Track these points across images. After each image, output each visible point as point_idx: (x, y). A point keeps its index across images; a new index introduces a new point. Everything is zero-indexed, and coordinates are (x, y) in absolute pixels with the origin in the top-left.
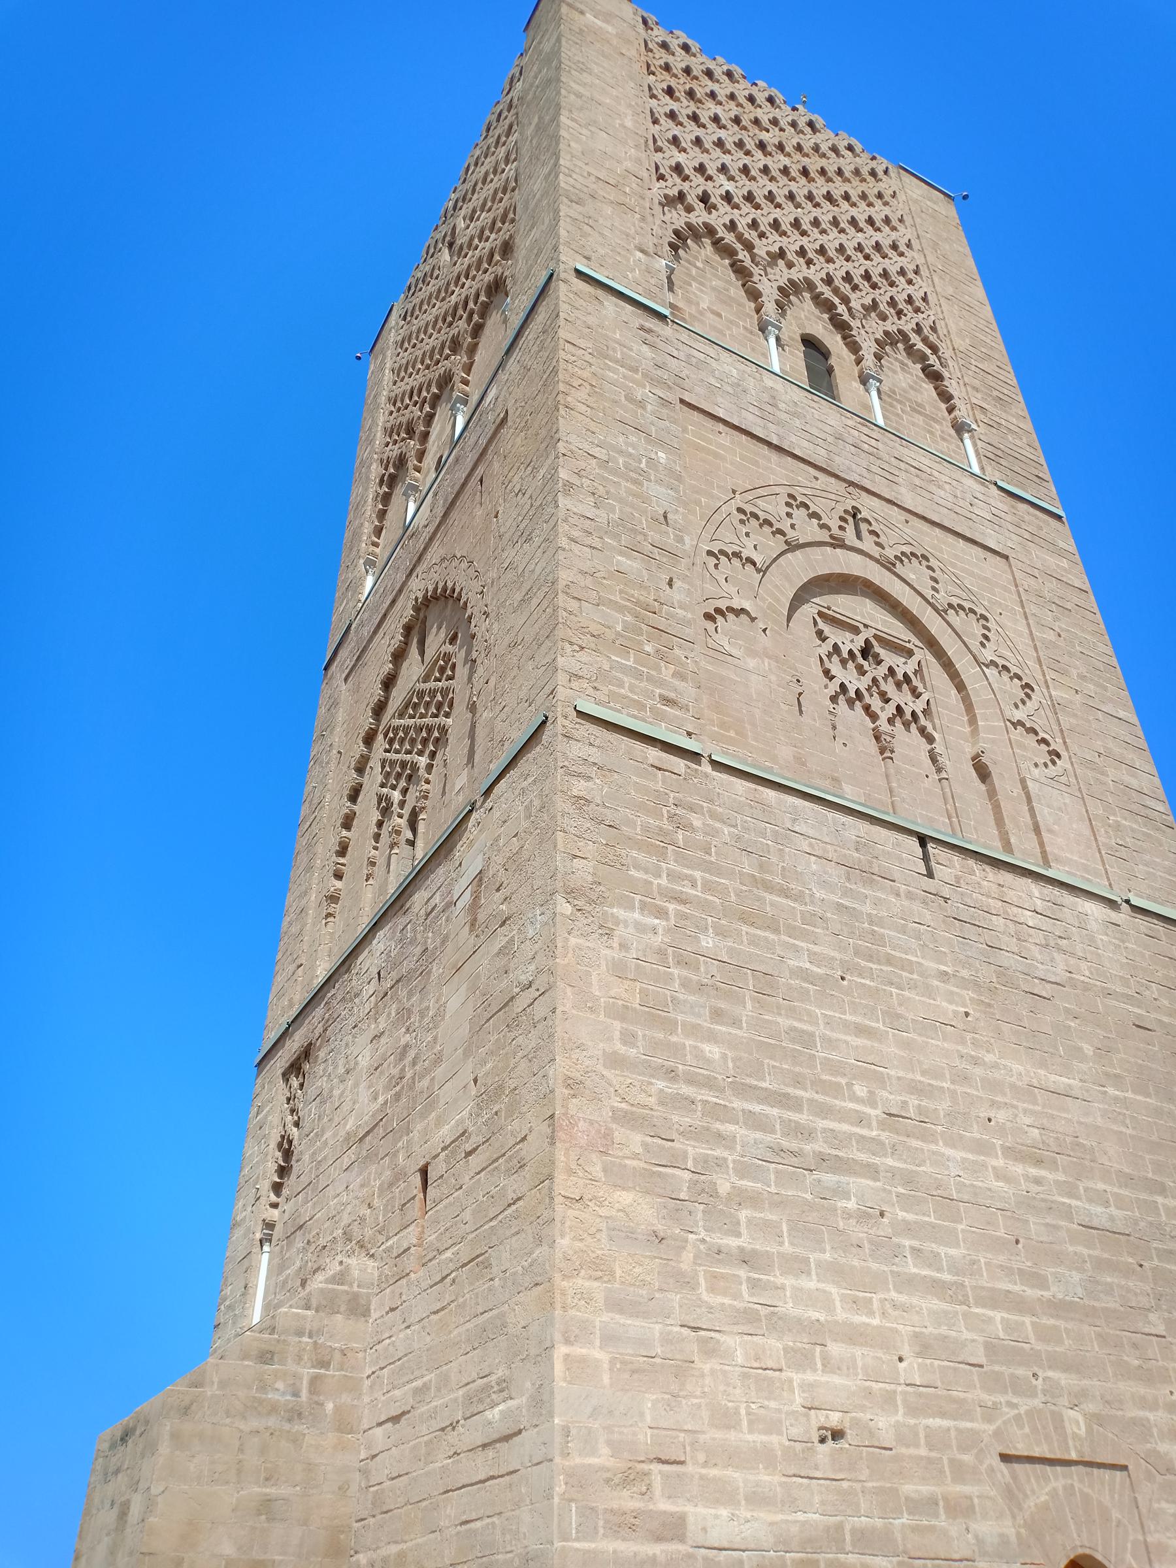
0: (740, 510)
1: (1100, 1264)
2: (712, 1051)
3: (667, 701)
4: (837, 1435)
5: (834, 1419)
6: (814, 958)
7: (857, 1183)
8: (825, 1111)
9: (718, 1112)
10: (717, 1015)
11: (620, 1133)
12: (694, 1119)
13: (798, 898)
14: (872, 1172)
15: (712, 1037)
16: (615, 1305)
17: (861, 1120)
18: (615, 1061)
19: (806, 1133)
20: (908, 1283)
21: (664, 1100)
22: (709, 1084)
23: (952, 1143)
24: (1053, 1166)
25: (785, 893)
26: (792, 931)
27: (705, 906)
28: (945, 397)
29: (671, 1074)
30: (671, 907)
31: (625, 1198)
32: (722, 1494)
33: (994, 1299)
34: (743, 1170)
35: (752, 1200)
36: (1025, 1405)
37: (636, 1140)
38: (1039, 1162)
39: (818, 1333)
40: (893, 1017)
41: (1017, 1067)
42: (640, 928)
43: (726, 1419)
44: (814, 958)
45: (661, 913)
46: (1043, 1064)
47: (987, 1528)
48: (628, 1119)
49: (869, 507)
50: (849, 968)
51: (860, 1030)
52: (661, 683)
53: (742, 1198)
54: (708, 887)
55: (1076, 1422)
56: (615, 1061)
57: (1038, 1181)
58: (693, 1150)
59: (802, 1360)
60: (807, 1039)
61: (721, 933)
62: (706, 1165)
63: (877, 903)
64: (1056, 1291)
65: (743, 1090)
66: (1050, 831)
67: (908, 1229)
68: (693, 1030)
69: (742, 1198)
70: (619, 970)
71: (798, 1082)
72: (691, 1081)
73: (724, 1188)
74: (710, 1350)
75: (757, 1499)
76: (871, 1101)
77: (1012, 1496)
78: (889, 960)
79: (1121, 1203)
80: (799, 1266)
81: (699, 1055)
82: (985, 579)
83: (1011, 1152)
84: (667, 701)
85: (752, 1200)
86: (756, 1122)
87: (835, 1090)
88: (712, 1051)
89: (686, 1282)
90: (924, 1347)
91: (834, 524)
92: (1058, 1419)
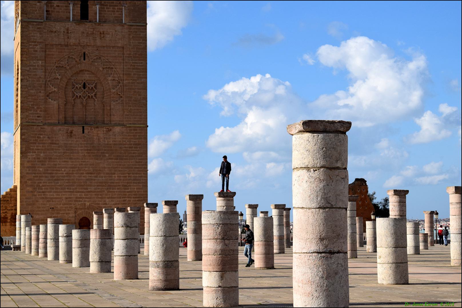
0: (57, 67)
1: (98, 186)
2: (41, 169)
3: (38, 117)
4: (53, 208)
5: (52, 207)
6: (59, 153)
7: (59, 182)
8: (56, 173)
9: (40, 177)
10: (42, 165)
11: (28, 181)
12: (38, 178)
13: (58, 144)
14: (63, 180)
15: (41, 168)
16: (26, 198)
17: (62, 173)
18: (27, 173)
19: (54, 177)
20: (66, 192)
21: (34, 177)
22: (40, 173)
23: (76, 174)
24: (94, 174)
25: (55, 144)
26: (56, 149)
27: (42, 150)
29: (35, 174)
30: (37, 151)
31: (28, 188)
32: (38, 214)
34: (44, 183)
35: (45, 186)
36: (80, 203)
37: (29, 182)
38: (91, 174)
39: (51, 198)
40: (71, 158)
41: (91, 161)
42: (32, 155)
44: (59, 153)
45: (35, 152)
46: (97, 159)
47: (71, 215)
48: (29, 180)
50: (64, 153)
51: (65, 161)
52: (37, 114)
53: (43, 186)
54: (42, 146)
56: (27, 173)
57: (90, 177)
58: (37, 182)
60: (56, 165)
61: (44, 153)
62: (39, 183)
63: (72, 141)
64: (89, 190)
65: (44, 173)
66: (114, 115)
67: (67, 186)
68: (39, 167)
69: (43, 186)
70: (28, 162)
71: (54, 170)
72: (38, 174)
73: (41, 185)
74: (37, 201)
75: (42, 214)
76: (65, 171)
77: (75, 212)
78: (72, 150)
79: (105, 177)
80: (51, 192)
81: (39, 170)
82: (115, 57)
83: (88, 173)
84: (38, 117)
85: (45, 186)
86: (46, 177)
87: (59, 171)
88: (41, 169)
90: (66, 198)
91: (78, 60)
92: (85, 204)
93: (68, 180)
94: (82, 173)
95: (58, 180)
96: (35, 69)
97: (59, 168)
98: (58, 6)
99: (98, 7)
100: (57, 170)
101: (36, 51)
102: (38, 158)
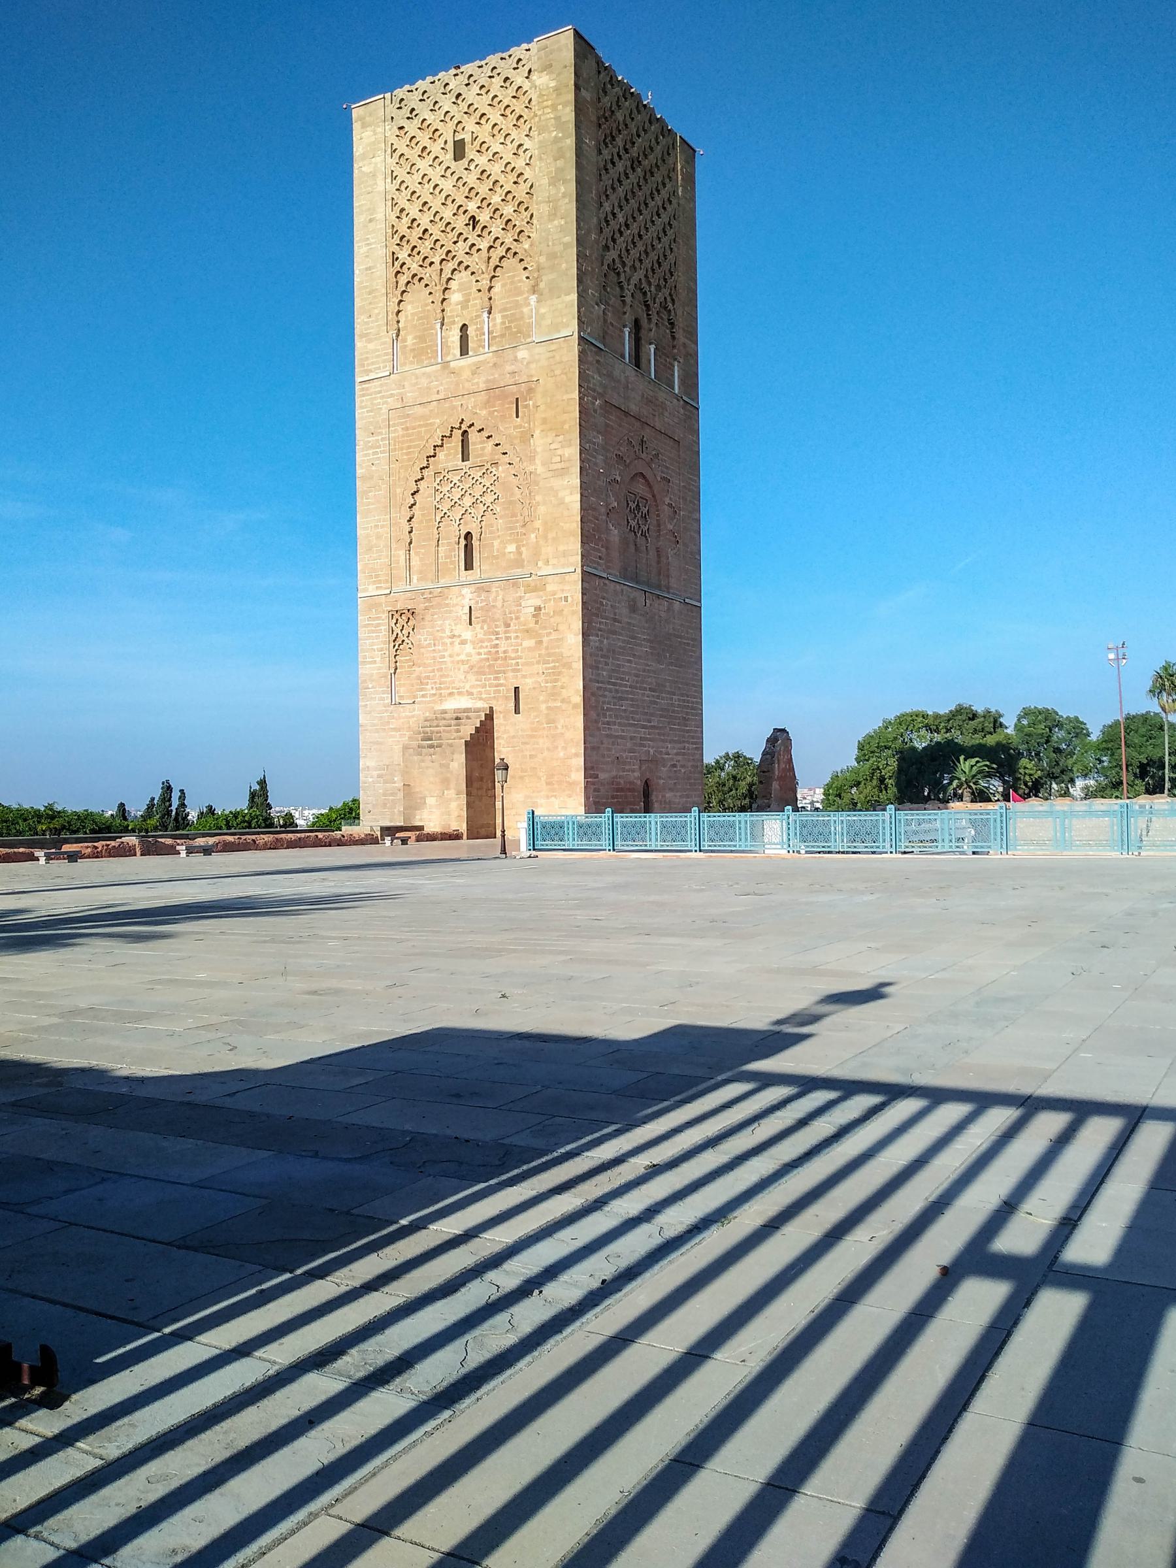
8: (621, 685)
17: (626, 686)
19: (617, 691)
28: (673, 338)
33: (644, 727)
34: (609, 703)
39: (617, 737)
43: (603, 756)
49: (647, 433)
55: (652, 751)
59: (613, 744)
65: (609, 683)
86: (611, 691)
89: (599, 729)
93: (632, 699)
94: (645, 689)
95: (621, 699)
96: (595, 450)
97: (624, 673)
98: (612, 324)
99: (652, 347)
100: (622, 679)
101: (595, 411)
102: (602, 650)
